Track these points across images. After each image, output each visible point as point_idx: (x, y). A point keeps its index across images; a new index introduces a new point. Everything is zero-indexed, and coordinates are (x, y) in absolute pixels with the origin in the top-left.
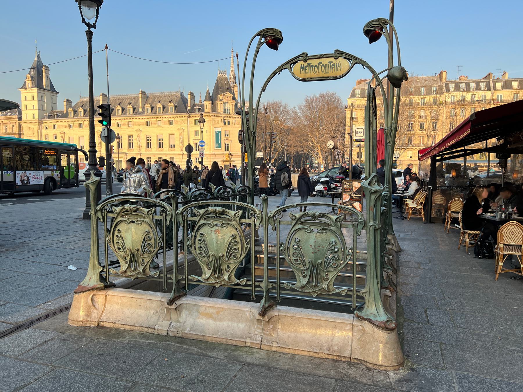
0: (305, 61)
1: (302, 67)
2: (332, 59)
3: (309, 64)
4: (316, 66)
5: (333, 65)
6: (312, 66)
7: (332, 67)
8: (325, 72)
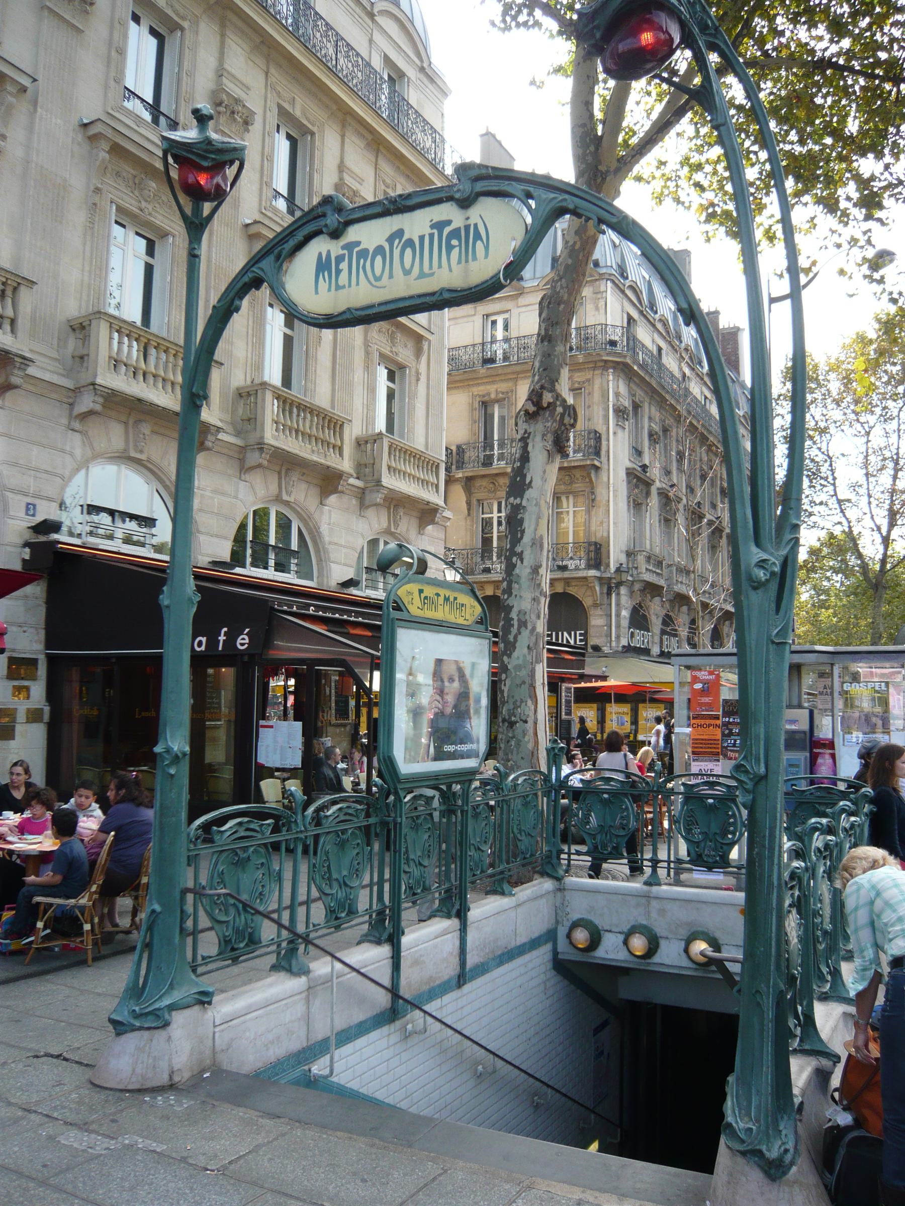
0: (336, 235)
1: (323, 266)
2: (446, 211)
3: (350, 247)
4: (380, 250)
5: (455, 233)
6: (364, 254)
7: (450, 248)
8: (416, 271)
